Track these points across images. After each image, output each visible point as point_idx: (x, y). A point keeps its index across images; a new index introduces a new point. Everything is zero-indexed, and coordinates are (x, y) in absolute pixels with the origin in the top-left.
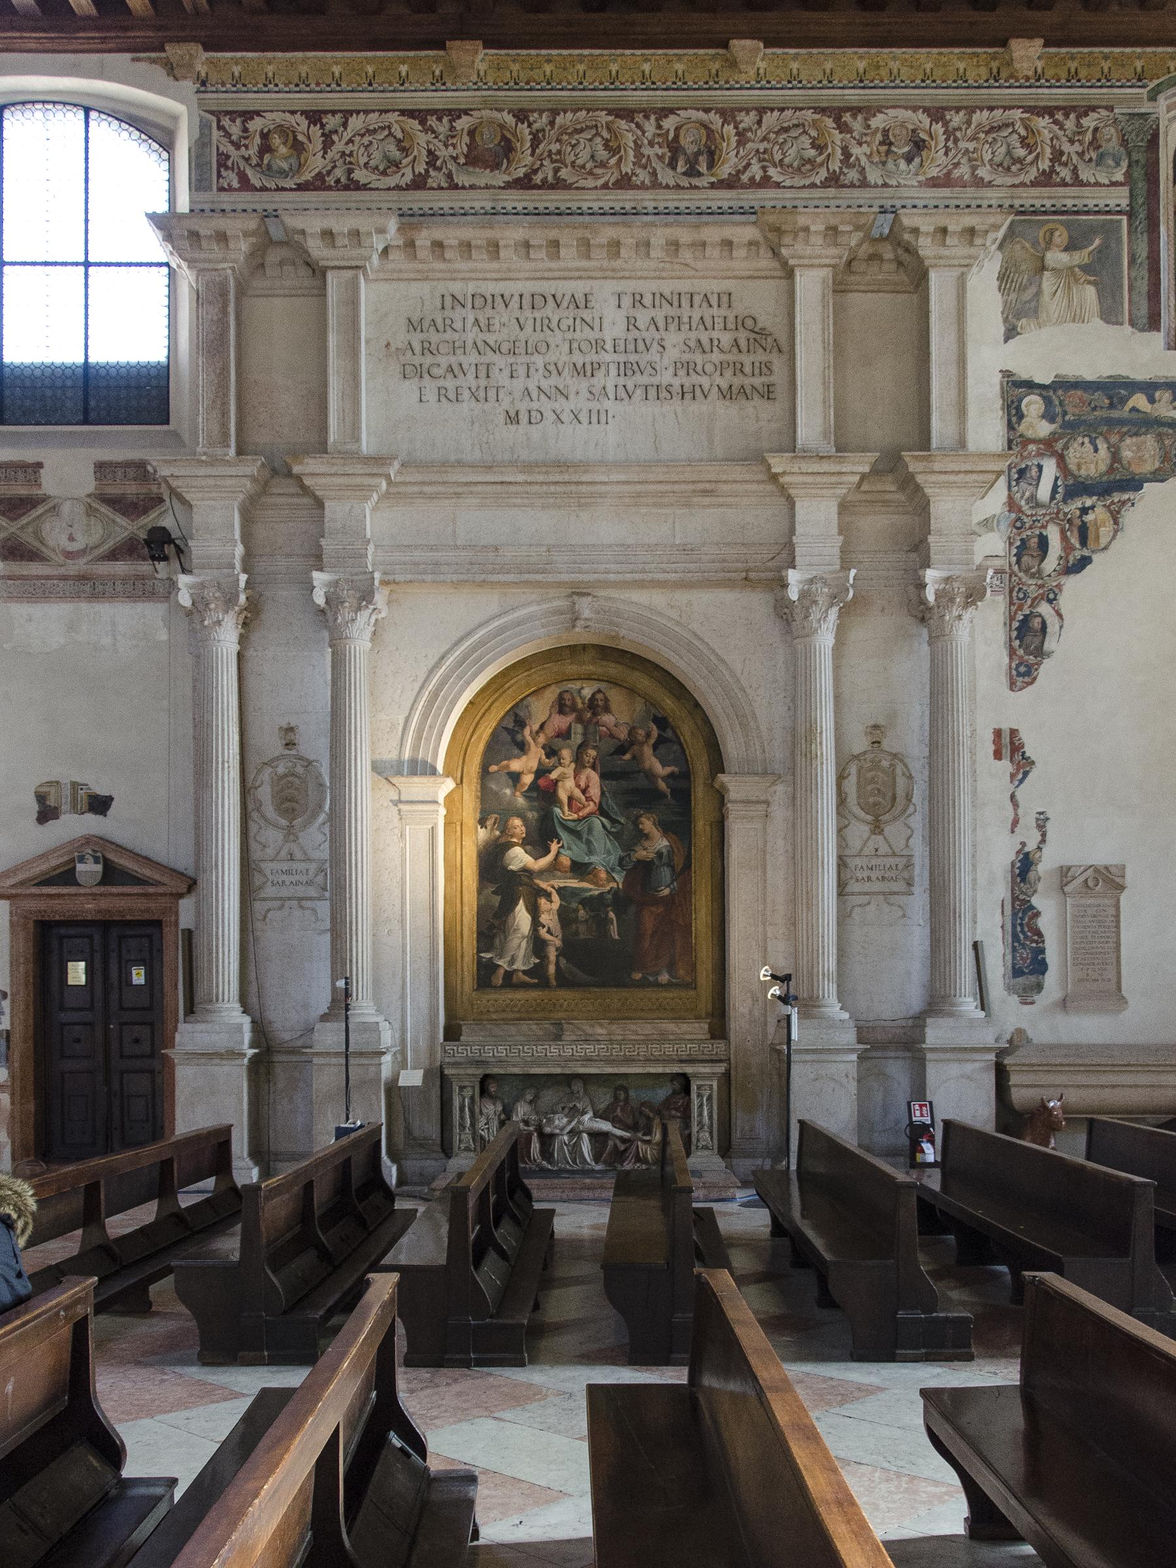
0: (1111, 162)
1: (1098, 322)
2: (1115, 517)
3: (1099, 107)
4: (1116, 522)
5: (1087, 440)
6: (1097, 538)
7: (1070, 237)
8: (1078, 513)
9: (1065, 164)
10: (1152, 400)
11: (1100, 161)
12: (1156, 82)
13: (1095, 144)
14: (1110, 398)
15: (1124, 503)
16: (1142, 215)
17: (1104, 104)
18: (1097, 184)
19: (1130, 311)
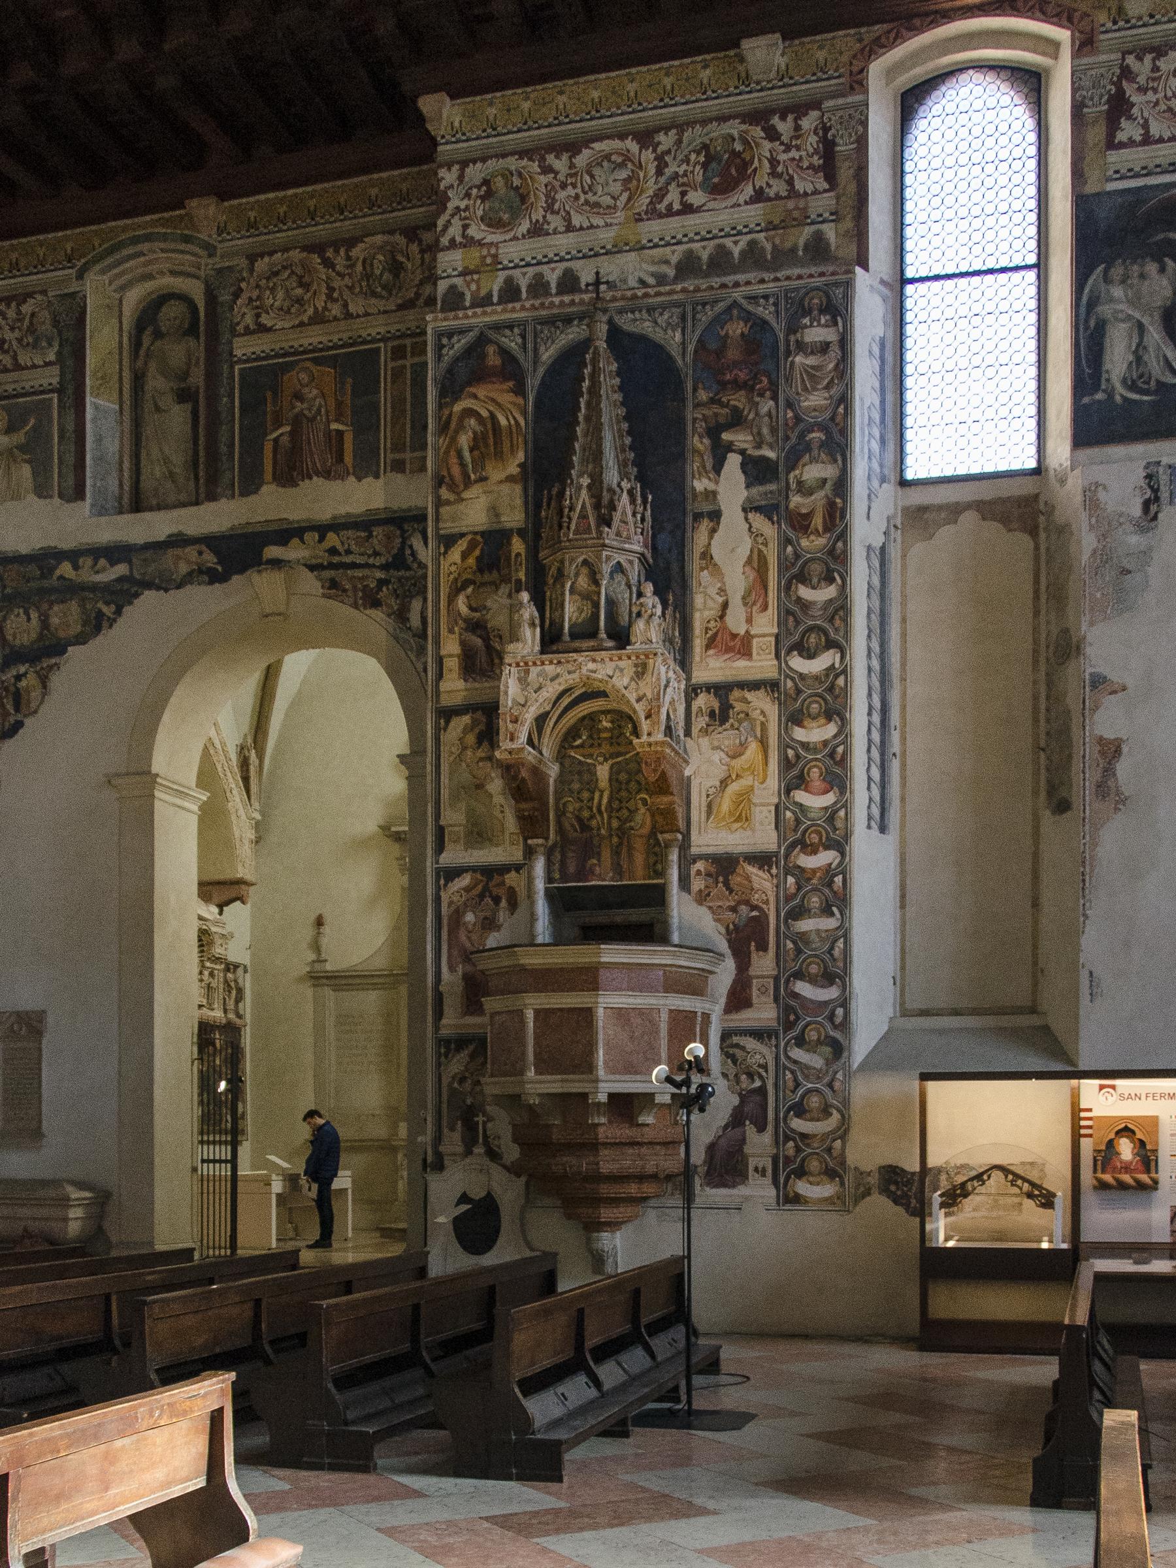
0: (44, 344)
1: (32, 498)
2: (44, 681)
3: (35, 293)
4: (45, 687)
5: (21, 611)
6: (29, 702)
7: (9, 421)
8: (13, 680)
9: (7, 352)
10: (76, 567)
11: (35, 345)
12: (83, 261)
13: (32, 329)
14: (41, 568)
15: (51, 668)
16: (70, 391)
17: (40, 288)
18: (34, 366)
19: (59, 483)
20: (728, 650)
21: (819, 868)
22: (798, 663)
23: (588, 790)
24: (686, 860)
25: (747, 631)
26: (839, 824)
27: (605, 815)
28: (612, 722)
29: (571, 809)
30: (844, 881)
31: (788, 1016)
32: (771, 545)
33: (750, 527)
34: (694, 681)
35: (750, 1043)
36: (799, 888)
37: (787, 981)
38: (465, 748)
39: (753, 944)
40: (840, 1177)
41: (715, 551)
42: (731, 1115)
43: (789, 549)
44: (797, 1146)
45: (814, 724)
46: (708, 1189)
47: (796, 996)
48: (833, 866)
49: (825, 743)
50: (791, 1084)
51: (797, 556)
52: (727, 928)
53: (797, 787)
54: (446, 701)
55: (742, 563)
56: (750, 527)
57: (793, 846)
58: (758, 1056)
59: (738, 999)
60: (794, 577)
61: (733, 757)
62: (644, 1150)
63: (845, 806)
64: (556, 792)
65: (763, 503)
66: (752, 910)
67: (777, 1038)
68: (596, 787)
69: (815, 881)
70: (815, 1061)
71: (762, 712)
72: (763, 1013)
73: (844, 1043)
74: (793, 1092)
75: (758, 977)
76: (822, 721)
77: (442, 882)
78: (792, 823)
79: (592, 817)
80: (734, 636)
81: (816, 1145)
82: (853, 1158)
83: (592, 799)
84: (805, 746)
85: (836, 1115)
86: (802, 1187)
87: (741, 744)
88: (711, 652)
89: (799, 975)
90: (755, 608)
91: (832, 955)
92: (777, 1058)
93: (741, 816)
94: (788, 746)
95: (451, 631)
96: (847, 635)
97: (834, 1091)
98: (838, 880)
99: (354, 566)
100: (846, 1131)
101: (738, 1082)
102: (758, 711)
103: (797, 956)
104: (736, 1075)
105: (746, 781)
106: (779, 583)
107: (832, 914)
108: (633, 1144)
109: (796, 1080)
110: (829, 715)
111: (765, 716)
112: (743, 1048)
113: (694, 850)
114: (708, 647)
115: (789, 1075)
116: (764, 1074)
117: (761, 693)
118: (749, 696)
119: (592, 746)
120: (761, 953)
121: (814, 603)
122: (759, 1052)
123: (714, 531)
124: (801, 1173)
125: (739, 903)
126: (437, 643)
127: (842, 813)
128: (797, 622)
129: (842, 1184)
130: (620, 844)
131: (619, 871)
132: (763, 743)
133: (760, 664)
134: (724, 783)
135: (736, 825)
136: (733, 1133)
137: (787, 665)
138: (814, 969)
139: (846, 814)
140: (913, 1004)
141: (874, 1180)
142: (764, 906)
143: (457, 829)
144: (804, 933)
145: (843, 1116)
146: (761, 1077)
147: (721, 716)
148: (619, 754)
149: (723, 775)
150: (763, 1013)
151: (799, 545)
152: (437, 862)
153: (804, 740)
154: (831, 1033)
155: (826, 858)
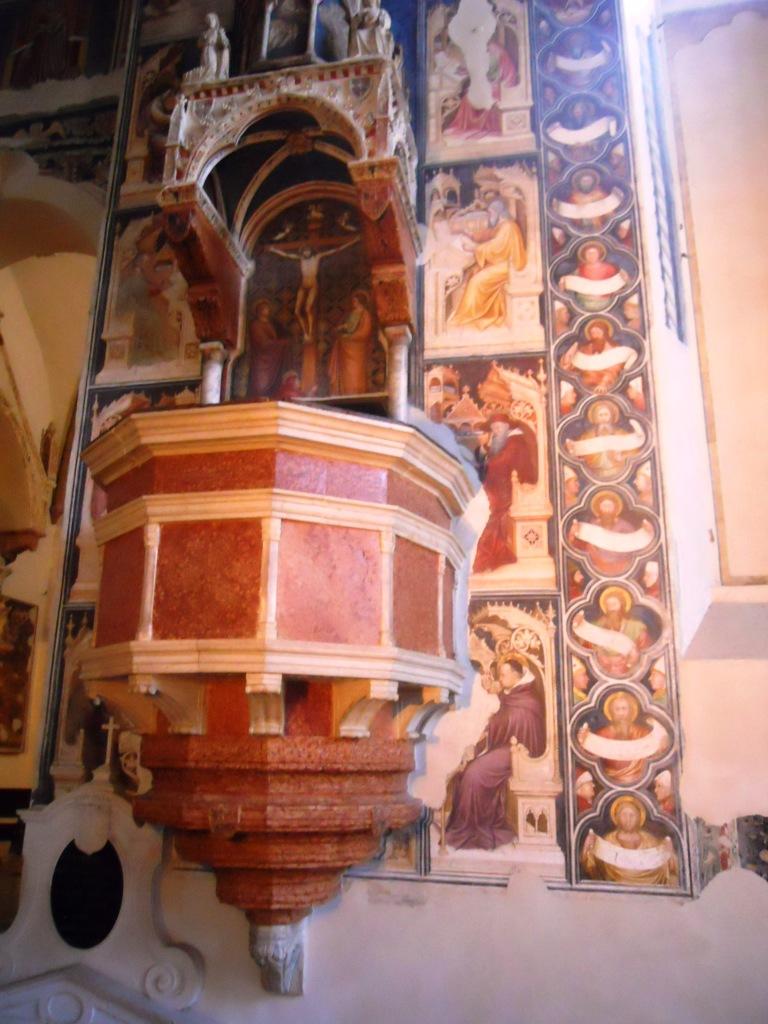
20: (470, 127)
21: (606, 370)
22: (561, 135)
24: (419, 365)
25: (494, 107)
26: (631, 313)
27: (310, 319)
28: (323, 212)
29: (266, 311)
30: (646, 386)
31: (571, 575)
32: (521, 23)
34: (428, 162)
35: (514, 616)
36: (579, 397)
37: (568, 525)
38: (140, 252)
39: (515, 473)
40: (673, 836)
42: (488, 729)
43: (543, 24)
44: (595, 781)
45: (588, 198)
46: (449, 849)
47: (582, 545)
48: (627, 367)
49: (604, 219)
50: (581, 680)
53: (569, 272)
54: (124, 204)
56: (494, 9)
57: (567, 343)
58: (527, 636)
59: (496, 550)
61: (481, 241)
62: (348, 785)
63: (638, 290)
67: (556, 607)
69: (601, 387)
70: (618, 642)
71: (518, 190)
72: (533, 570)
73: (665, 616)
74: (586, 692)
75: (524, 519)
76: (599, 194)
77: (96, 406)
78: (564, 316)
80: (478, 112)
81: (628, 779)
82: (693, 803)
84: (577, 224)
85: (658, 733)
86: (607, 850)
87: (490, 226)
88: (449, 131)
89: (584, 516)
90: (503, 84)
91: (634, 487)
93: (493, 307)
95: (140, 134)
96: (624, 98)
97: (652, 691)
98: (636, 385)
99: (73, 147)
100: (678, 757)
101: (497, 676)
102: (512, 189)
103: (581, 489)
104: (494, 665)
106: (532, 57)
107: (630, 430)
108: (331, 773)
109: (589, 673)
110: (606, 189)
112: (504, 624)
113: (429, 354)
115: (578, 666)
116: (538, 663)
117: (515, 169)
118: (499, 173)
120: (526, 486)
121: (578, 73)
122: (529, 630)
123: (450, 16)
124: (605, 826)
125: (493, 419)
126: (123, 147)
127: (634, 300)
129: (677, 847)
130: (328, 352)
132: (521, 224)
134: (468, 272)
135: (486, 322)
137: (546, 135)
138: (607, 506)
139: (641, 300)
140: (740, 568)
141: (730, 842)
142: (530, 424)
143: (119, 343)
145: (670, 731)
146: (533, 668)
147: (464, 196)
148: (330, 247)
149: (467, 263)
150: (533, 570)
151: (555, 19)
152: (93, 383)
155: (615, 356)
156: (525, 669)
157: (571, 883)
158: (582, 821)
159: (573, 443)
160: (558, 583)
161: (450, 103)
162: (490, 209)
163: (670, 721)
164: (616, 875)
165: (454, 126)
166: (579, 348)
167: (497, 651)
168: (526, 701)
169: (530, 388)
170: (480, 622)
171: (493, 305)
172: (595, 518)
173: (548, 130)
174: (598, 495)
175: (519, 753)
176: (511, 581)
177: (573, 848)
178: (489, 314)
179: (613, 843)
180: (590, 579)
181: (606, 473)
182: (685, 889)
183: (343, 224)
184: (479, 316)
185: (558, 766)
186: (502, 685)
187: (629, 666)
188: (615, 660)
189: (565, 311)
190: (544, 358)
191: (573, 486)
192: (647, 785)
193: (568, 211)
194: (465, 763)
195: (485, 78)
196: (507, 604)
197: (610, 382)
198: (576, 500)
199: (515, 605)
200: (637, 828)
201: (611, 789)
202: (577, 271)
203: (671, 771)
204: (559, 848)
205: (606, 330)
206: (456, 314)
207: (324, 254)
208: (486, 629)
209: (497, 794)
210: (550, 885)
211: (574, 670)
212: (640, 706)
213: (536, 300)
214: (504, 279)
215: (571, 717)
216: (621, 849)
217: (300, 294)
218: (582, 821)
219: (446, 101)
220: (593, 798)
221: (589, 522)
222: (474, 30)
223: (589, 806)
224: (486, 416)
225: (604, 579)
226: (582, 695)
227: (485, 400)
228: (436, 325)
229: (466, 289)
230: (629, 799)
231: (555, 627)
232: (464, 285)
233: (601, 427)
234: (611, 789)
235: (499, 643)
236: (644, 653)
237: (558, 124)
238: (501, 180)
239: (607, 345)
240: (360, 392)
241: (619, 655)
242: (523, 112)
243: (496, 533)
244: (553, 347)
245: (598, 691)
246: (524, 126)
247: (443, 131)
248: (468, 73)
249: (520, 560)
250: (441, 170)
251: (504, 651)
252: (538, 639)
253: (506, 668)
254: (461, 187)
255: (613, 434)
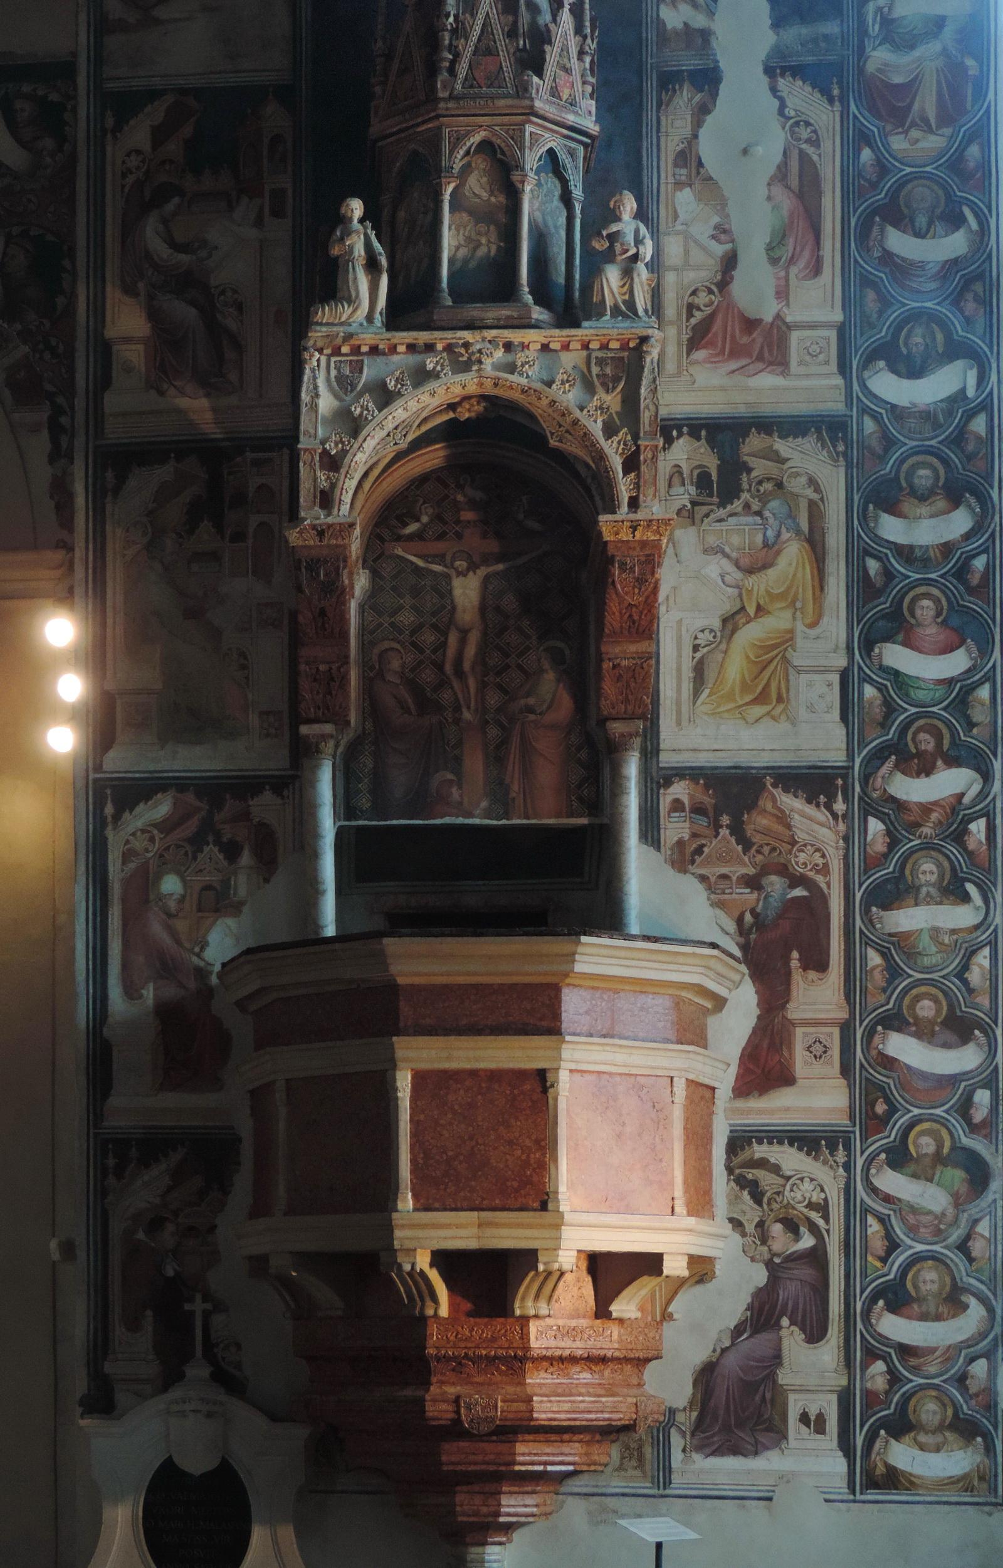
21: (935, 803)
23: (434, 627)
25: (778, 316)
27: (472, 683)
29: (396, 664)
31: (872, 1104)
32: (827, 145)
33: (783, 106)
34: (663, 412)
35: (790, 1159)
36: (893, 842)
37: (870, 1034)
39: (795, 955)
41: (706, 149)
42: (750, 1307)
43: (866, 154)
45: (924, 510)
47: (888, 1063)
50: (878, 1245)
51: (883, 169)
52: (740, 921)
53: (888, 638)
55: (766, 179)
56: (783, 106)
57: (879, 756)
58: (807, 1186)
60: (875, 211)
61: (750, 571)
64: (363, 629)
65: (810, 59)
66: (792, 886)
67: (848, 1147)
68: (451, 621)
69: (927, 830)
71: (812, 482)
74: (884, 1260)
78: (878, 711)
79: (443, 683)
80: (750, 324)
81: (932, 1369)
83: (444, 645)
84: (905, 553)
87: (766, 545)
88: (700, 355)
89: (895, 1021)
90: (794, 270)
92: (848, 1191)
94: (867, 553)
97: (971, 1260)
102: (803, 480)
103: (890, 982)
104: (760, 1225)
105: (778, 621)
106: (845, 221)
111: (817, 490)
112: (776, 1169)
113: (667, 759)
114: (693, 344)
115: (874, 1226)
116: (821, 1222)
117: (809, 443)
118: (782, 447)
119: (441, 537)
120: (812, 975)
125: (765, 871)
128: (885, 302)
129: (989, 1449)
131: (502, 801)
133: (805, 383)
134: (731, 623)
135: (758, 710)
136: (756, 1345)
137: (863, 385)
138: (926, 1009)
142: (820, 879)
144: (906, 935)
146: (814, 1229)
149: (728, 607)
151: (887, 146)
153: (901, 540)
154: (966, 1141)
156: (802, 1229)
157: (854, 1493)
158: (872, 1420)
159: (882, 913)
160: (852, 1118)
161: (702, 299)
162: (767, 514)
163: (991, 1297)
164: (912, 1483)
165: (704, 347)
166: (897, 766)
167: (765, 1206)
168: (806, 1272)
169: (822, 825)
170: (741, 1167)
171: (768, 685)
172: (908, 1024)
173: (866, 374)
174: (914, 992)
175: (792, 1339)
176: (787, 1109)
177: (859, 1453)
178: (762, 698)
179: (909, 1446)
180: (896, 1110)
181: (926, 961)
182: (996, 1497)
183: (521, 516)
184: (749, 698)
185: (842, 1354)
186: (770, 1250)
187: (942, 1227)
188: (925, 1219)
189: (878, 702)
190: (845, 777)
191: (879, 978)
192: (956, 1377)
193: (891, 528)
194: (719, 1350)
195: (764, 257)
196: (780, 1143)
197: (940, 822)
198: (882, 998)
199: (791, 1144)
200: (940, 1428)
201: (911, 1381)
202: (900, 637)
203: (988, 1359)
204: (840, 1454)
205: (939, 738)
206: (708, 696)
207: (491, 569)
208: (750, 1176)
209: (762, 1388)
210: (828, 1497)
211: (869, 1231)
212: (953, 1279)
213: (835, 678)
214: (788, 639)
215: (862, 1293)
216: (920, 1452)
217: (453, 639)
218: (872, 1420)
219: (694, 293)
220: (887, 1393)
221: (899, 1030)
222: (745, 152)
223: (882, 1402)
224: (754, 865)
225: (916, 1111)
226: (878, 1264)
227: (754, 840)
228: (679, 713)
229: (726, 652)
230: (934, 1393)
231: (845, 1174)
232: (723, 646)
233: (924, 890)
234: (911, 1381)
235: (768, 1194)
236: (964, 1211)
237: (882, 364)
238: (784, 461)
239: (939, 763)
240: (557, 816)
241: (930, 1212)
242: (826, 333)
243: (765, 1044)
244: (858, 761)
245: (899, 1259)
246: (827, 363)
247: (688, 354)
248: (733, 241)
249: (800, 1082)
250: (685, 429)
251: (775, 1206)
252: (822, 1190)
253: (777, 1229)
254: (719, 466)
255: (941, 903)
